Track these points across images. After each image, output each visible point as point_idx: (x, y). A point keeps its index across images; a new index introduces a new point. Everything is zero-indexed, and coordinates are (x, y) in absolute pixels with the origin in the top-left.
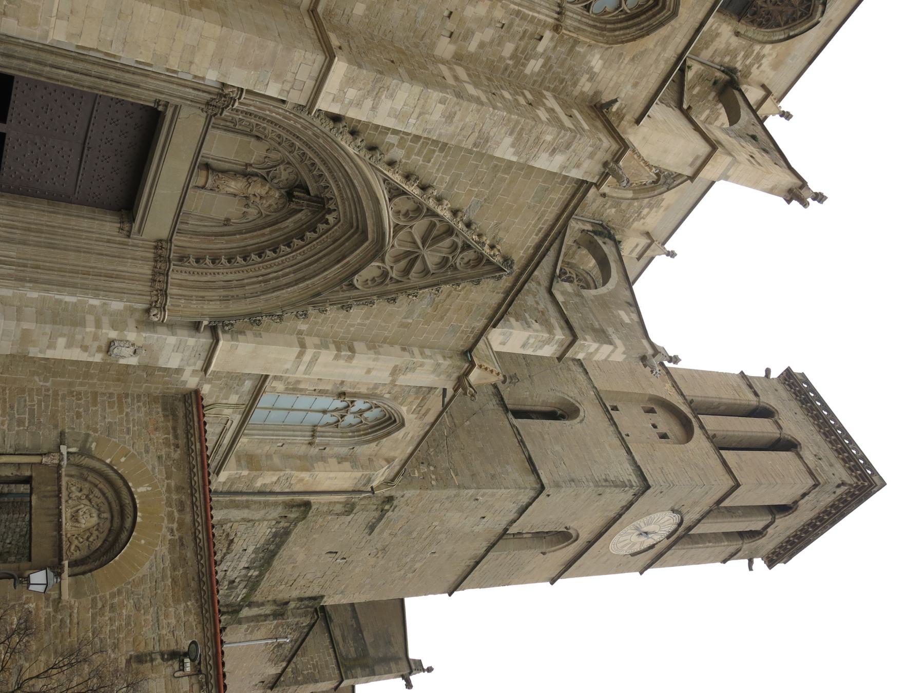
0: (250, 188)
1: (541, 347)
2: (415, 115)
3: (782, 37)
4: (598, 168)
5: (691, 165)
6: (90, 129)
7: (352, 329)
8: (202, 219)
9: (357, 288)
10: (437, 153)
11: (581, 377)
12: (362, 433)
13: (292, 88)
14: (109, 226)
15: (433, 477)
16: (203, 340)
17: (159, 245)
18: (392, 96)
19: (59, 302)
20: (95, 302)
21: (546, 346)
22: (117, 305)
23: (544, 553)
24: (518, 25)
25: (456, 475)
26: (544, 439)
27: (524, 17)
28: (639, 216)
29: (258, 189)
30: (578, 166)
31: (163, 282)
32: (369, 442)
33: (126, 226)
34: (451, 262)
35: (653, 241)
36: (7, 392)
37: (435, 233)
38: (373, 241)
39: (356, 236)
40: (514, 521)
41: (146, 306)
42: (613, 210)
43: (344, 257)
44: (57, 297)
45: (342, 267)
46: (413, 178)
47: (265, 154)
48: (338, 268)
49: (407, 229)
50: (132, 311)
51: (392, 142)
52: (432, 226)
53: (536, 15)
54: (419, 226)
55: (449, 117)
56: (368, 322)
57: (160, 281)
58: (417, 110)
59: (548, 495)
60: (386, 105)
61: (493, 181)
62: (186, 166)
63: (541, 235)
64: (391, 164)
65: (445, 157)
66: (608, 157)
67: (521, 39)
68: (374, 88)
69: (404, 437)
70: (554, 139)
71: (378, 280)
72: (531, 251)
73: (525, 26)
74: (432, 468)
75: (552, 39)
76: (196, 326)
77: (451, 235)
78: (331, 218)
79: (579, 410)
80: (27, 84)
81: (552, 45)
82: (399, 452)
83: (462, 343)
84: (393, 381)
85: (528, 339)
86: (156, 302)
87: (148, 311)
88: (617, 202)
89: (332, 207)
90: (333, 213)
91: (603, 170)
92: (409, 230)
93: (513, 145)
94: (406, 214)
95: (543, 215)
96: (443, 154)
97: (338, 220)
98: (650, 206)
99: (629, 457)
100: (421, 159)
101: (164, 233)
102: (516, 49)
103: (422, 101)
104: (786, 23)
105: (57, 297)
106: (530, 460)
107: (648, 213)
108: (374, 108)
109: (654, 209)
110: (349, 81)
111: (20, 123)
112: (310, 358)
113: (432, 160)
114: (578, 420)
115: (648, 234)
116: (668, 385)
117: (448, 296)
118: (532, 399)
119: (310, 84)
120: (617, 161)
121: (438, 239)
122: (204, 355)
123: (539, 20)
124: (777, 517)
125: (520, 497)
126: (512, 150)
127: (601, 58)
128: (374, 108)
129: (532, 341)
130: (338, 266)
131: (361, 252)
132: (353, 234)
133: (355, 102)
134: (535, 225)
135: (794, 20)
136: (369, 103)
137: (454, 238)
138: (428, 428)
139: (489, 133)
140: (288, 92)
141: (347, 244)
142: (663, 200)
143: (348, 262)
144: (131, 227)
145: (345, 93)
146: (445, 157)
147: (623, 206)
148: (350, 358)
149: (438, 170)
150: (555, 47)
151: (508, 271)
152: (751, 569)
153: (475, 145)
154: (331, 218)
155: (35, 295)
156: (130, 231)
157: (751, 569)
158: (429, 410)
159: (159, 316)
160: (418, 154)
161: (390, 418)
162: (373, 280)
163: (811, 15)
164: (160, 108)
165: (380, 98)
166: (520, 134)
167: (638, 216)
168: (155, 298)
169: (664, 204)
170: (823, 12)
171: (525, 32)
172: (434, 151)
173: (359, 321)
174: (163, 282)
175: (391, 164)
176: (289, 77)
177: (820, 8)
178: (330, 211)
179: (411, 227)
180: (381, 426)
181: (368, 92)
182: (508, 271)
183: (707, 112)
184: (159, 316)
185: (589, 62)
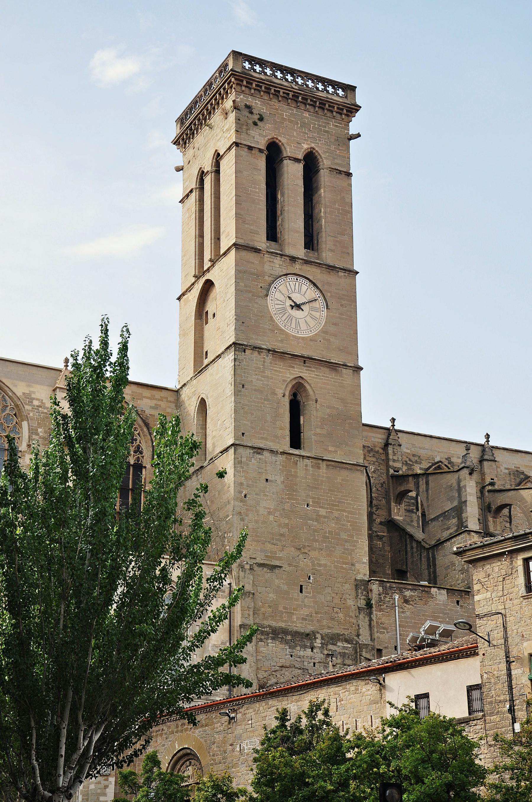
23: (316, 401)
40: (272, 451)
42: (40, 430)
88: (32, 431)
109: (33, 396)
124: (285, 156)
142: (24, 394)
152: (359, 135)
157: (359, 135)
167: (40, 407)
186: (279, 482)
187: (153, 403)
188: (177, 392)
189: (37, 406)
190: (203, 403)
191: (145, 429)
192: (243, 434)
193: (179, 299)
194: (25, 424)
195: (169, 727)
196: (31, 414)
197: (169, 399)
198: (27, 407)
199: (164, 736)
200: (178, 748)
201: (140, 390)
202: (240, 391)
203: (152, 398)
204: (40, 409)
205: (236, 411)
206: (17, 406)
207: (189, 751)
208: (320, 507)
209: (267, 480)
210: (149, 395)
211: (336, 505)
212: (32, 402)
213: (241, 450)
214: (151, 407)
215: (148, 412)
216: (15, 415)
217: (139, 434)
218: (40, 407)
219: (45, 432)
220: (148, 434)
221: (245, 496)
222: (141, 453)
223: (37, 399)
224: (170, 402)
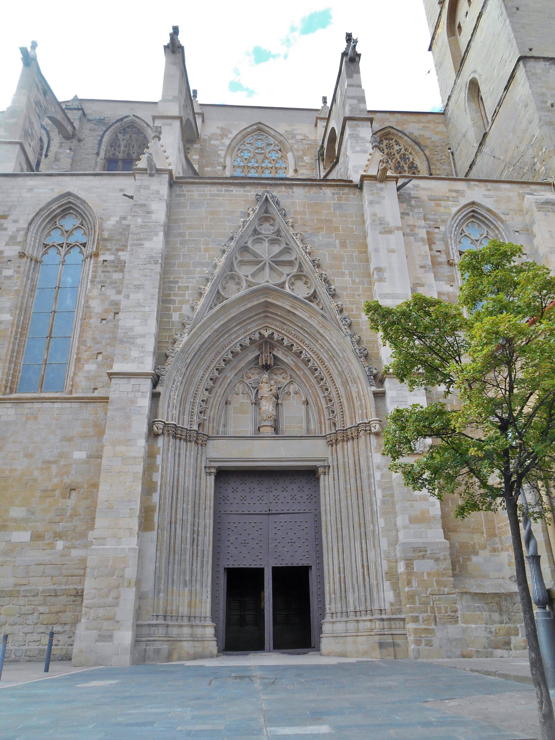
0: (265, 395)
1: (363, 139)
2: (142, 309)
4: (155, 179)
5: (170, 125)
6: (254, 513)
7: (357, 280)
8: (308, 421)
9: (315, 291)
10: (180, 284)
11: (453, 99)
12: (497, 232)
13: (139, 391)
14: (325, 482)
15: (540, 154)
17: (333, 443)
18: (131, 329)
19: (384, 502)
20: (378, 476)
21: (361, 135)
24: (100, 278)
25: (534, 136)
26: (494, 89)
27: (94, 277)
28: (306, 138)
29: (265, 390)
30: (158, 192)
31: (351, 431)
32: (502, 222)
33: (321, 470)
34: (274, 236)
35: (317, 118)
36: (500, 525)
37: (251, 258)
38: (266, 297)
39: (271, 310)
41: (373, 437)
42: (305, 158)
43: (289, 312)
44: (379, 504)
45: (296, 309)
46: (200, 291)
47: (241, 395)
48: (299, 311)
49: (250, 279)
51: (178, 316)
52: (242, 263)
53: (91, 271)
54: (244, 272)
55: (138, 287)
56: (347, 272)
57: (352, 434)
58: (137, 309)
60: (139, 330)
61: (193, 240)
62: (257, 443)
63: (232, 188)
64: (193, 308)
65: (181, 278)
66: (146, 177)
67: (109, 272)
68: (127, 342)
69: (485, 196)
70: (140, 216)
71: (304, 279)
72: (248, 188)
73: (100, 273)
74: (536, 160)
75: (103, 254)
77: (247, 247)
78: (266, 334)
79: (470, 81)
80: (228, 559)
81: (107, 252)
82: (511, 194)
83: (352, 196)
84: (398, 228)
85: (357, 152)
86: (366, 430)
88: (298, 159)
89: (257, 336)
90: (262, 333)
91: (156, 175)
92: (249, 276)
93: (151, 240)
94: (238, 284)
95: (214, 195)
96: (180, 280)
97: (266, 328)
98: (294, 136)
99: (483, 12)
100: (187, 292)
101: (322, 443)
102: (115, 271)
103: (130, 309)
104: (142, 133)
105: (379, 504)
106: (507, 88)
107: (300, 134)
108: (143, 336)
109: (295, 132)
110: (125, 358)
111: (261, 559)
112: (388, 300)
113: (186, 285)
114: (476, 76)
115: (316, 126)
116: (439, 31)
117: (304, 225)
118: (477, 122)
119: (133, 381)
120: (146, 170)
121: (255, 255)
123: (94, 267)
126: (155, 239)
127: (109, 220)
128: (143, 336)
129: (358, 149)
130: (297, 313)
131: (279, 301)
132: (272, 313)
133: (141, 350)
134: (224, 196)
135: (139, 130)
136: (139, 341)
137: (249, 244)
138: (472, 183)
139: (145, 259)
140: (143, 392)
141: (280, 314)
142: (286, 131)
143: (291, 306)
144: (320, 466)
145: (135, 358)
146: (181, 278)
147: (300, 153)
148: (379, 270)
149: (193, 278)
150: (108, 250)
151: (266, 194)
153: (156, 263)
154: (266, 334)
156: (325, 467)
158: (450, 191)
159: (374, 425)
160: (183, 295)
161: (473, 216)
162: (306, 283)
163: (132, 122)
164: (213, 470)
165: (134, 336)
166: (141, 239)
167: (304, 140)
168: (362, 432)
169: (289, 129)
170: (126, 117)
171: (103, 272)
172: (179, 287)
173: (347, 278)
174: (351, 431)
175: (193, 308)
176: (131, 395)
177: (125, 120)
178: (261, 336)
179: (247, 276)
180: (483, 219)
181: (131, 344)
182: (266, 194)
183: (213, 142)
184: (374, 425)
185: (113, 225)
187: (420, 126)
188: (443, 114)
189: (301, 140)
191: (416, 147)
192: (531, 50)
193: (430, 49)
194: (290, 155)
196: (295, 146)
197: (437, 121)
198: (290, 141)
201: (405, 117)
202: (515, 13)
203: (419, 122)
204: (304, 141)
205: (514, 30)
206: (280, 142)
210: (416, 120)
212: (295, 137)
213: (531, 64)
214: (419, 129)
215: (416, 133)
216: (280, 150)
217: (410, 153)
218: (304, 140)
219: (312, 159)
220: (420, 151)
222: (416, 168)
223: (300, 134)
224: (439, 123)
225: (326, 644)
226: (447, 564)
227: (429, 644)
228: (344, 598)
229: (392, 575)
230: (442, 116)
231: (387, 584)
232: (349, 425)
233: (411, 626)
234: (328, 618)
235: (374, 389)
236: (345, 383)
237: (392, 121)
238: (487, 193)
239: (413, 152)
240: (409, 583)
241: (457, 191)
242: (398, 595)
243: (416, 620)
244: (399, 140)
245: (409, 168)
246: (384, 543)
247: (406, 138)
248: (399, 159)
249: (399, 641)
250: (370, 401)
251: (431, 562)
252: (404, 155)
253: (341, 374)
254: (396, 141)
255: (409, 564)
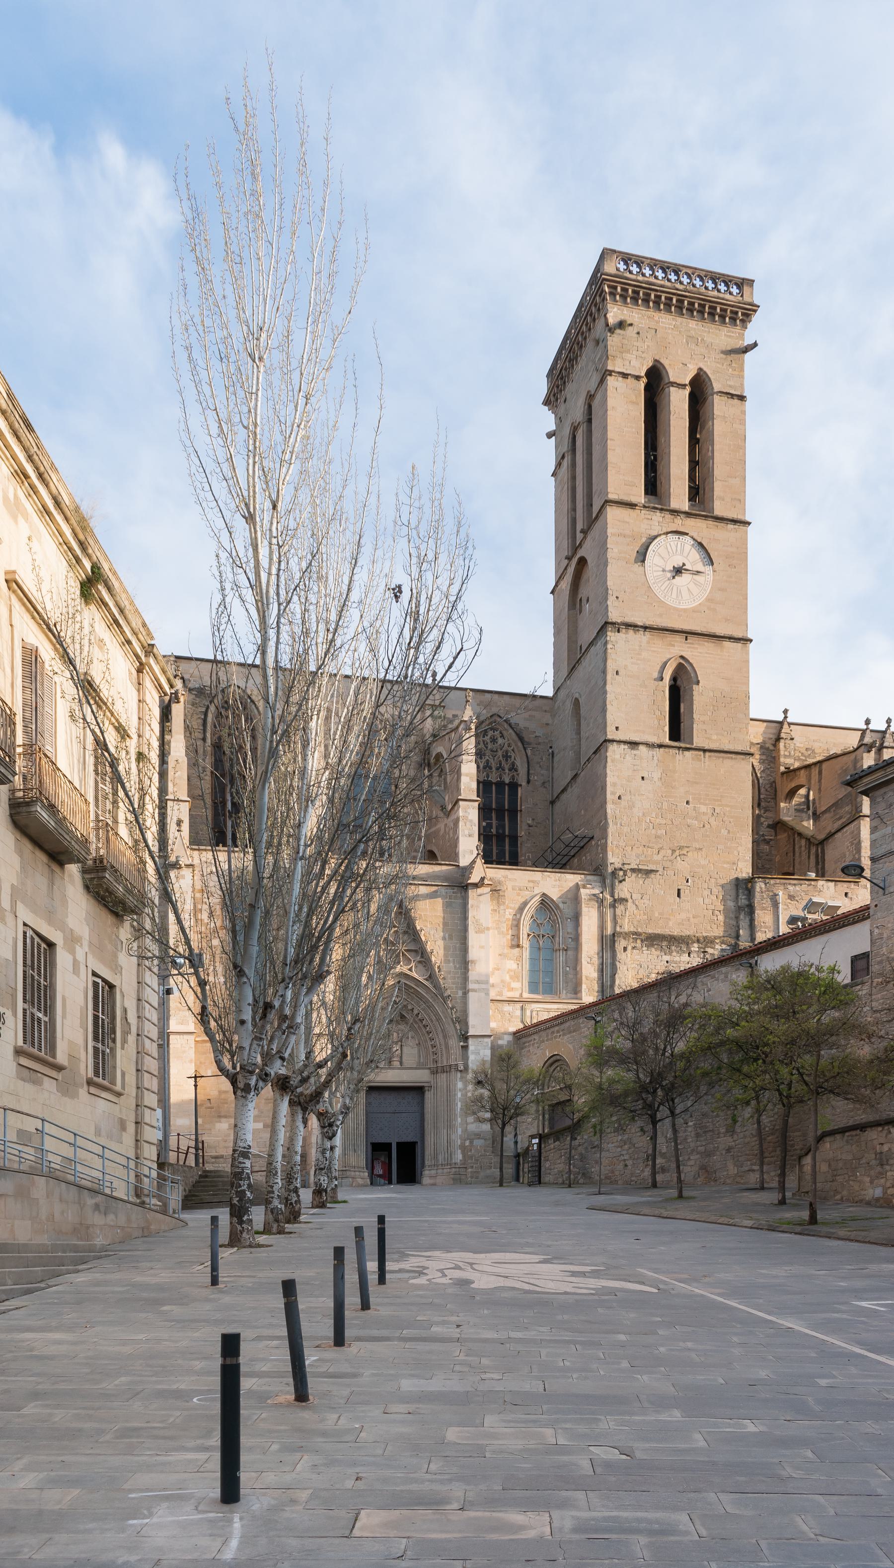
3: (253, 706)
8: (420, 1056)
14: (428, 1095)
16: (471, 1041)
17: (435, 1072)
19: (461, 1109)
20: (459, 1095)
22: (460, 1085)
33: (426, 1088)
50: (462, 1078)
59: (617, 728)
76: (465, 1048)
87: (461, 1071)
101: (427, 1072)
122: (480, 1039)
125: (618, 756)
155: (459, 1120)
186: (656, 779)
190: (576, 703)
195: (540, 1037)
199: (536, 1045)
200: (548, 1055)
207: (558, 1057)
208: (701, 803)
209: (643, 778)
211: (718, 800)
221: (619, 798)
225: (426, 1180)
226: (490, 1142)
227: (477, 1178)
228: (436, 1157)
229: (463, 1148)
230: (550, 701)
231: (459, 1151)
232: (445, 1064)
233: (470, 1170)
234: (427, 1168)
235: (462, 1044)
236: (445, 1037)
237: (502, 703)
238: (554, 883)
239: (516, 750)
240: (471, 1150)
241: (533, 882)
242: (464, 1156)
243: (472, 1167)
244: (504, 733)
245: (510, 770)
246: (460, 1131)
247: (511, 731)
248: (501, 758)
249: (463, 1177)
250: (459, 1052)
251: (483, 1141)
252: (507, 752)
253: (443, 1031)
254: (501, 733)
255: (471, 1142)
